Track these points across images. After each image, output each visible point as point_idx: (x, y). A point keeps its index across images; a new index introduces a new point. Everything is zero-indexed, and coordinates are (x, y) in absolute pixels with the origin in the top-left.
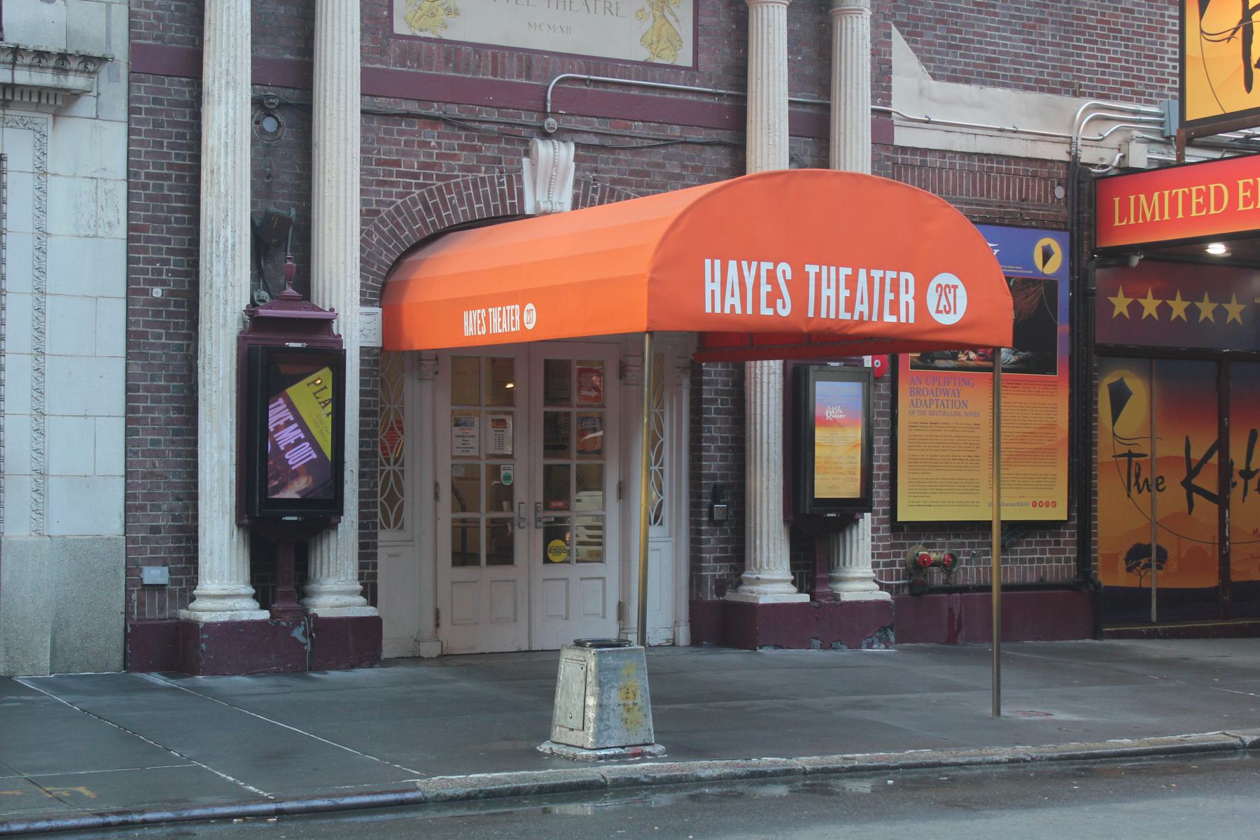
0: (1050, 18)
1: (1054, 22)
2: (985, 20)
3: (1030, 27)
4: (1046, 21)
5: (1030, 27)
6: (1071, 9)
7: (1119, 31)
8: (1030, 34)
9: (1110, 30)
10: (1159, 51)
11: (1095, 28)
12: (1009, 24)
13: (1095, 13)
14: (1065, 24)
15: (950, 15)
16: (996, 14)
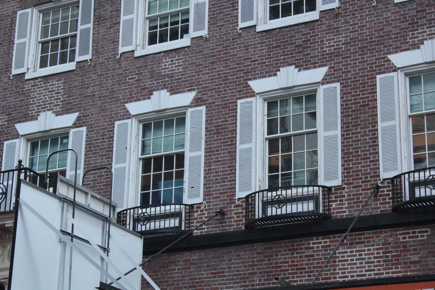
0: (258, 271)
1: (260, 273)
2: (218, 281)
3: (245, 278)
4: (256, 273)
5: (245, 278)
6: (271, 264)
7: (305, 268)
8: (246, 282)
9: (297, 269)
10: (331, 274)
11: (288, 270)
12: (233, 279)
13: (288, 262)
14: (268, 272)
15: (197, 282)
16: (225, 276)
